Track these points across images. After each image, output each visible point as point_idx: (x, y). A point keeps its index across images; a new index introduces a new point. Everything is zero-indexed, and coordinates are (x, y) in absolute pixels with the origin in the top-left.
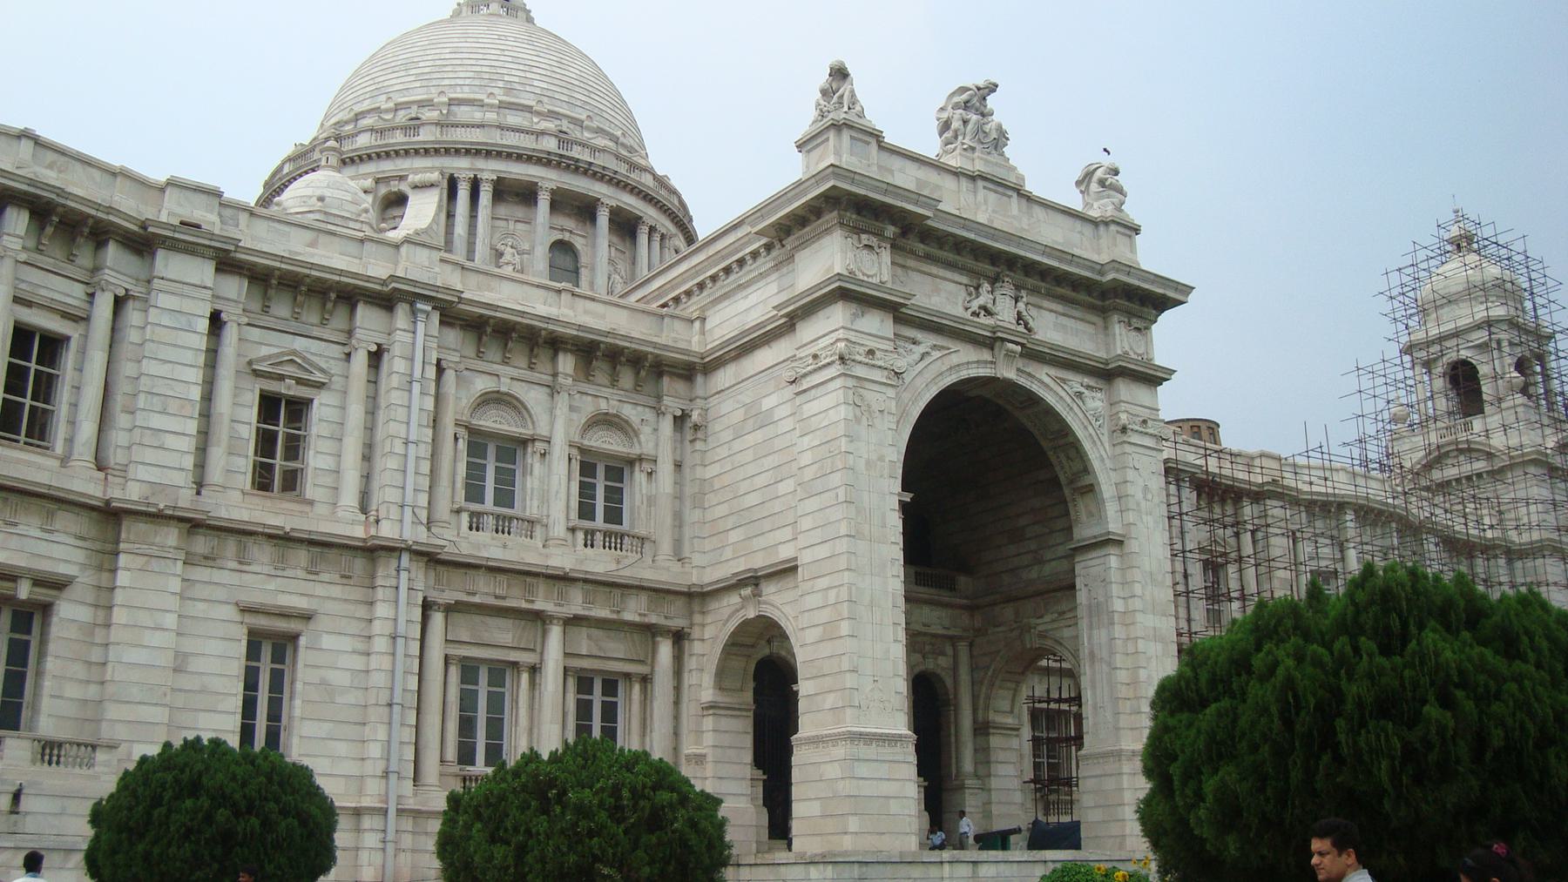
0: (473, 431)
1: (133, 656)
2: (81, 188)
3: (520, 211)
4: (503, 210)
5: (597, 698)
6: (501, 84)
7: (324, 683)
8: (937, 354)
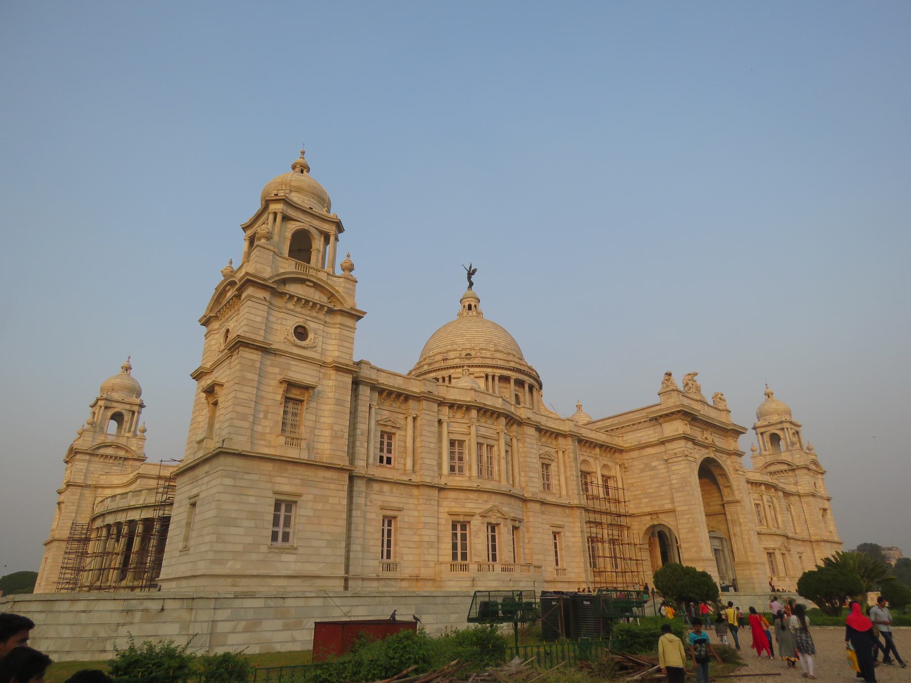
3: (504, 385)
4: (500, 385)
8: (699, 452)
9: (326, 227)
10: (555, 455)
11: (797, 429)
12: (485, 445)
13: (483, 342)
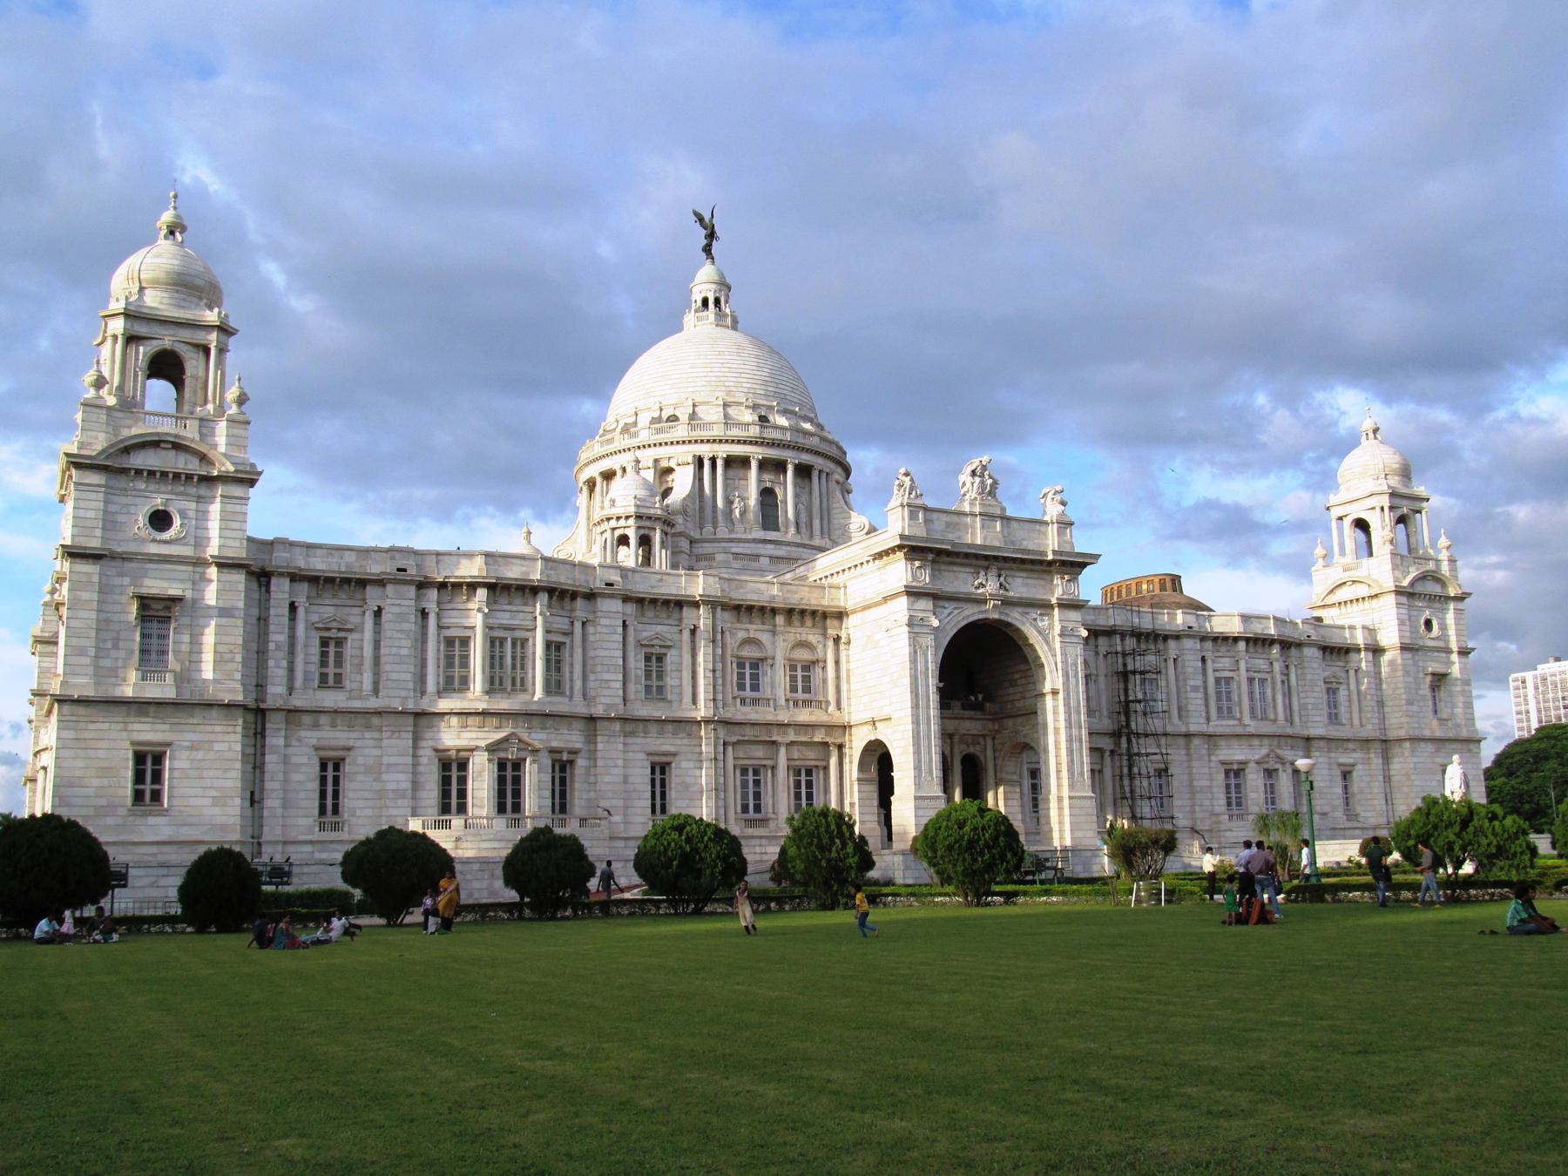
0: (737, 657)
1: (607, 779)
2: (564, 579)
3: (741, 473)
4: (731, 473)
5: (803, 778)
6: (723, 388)
7: (683, 782)
8: (956, 612)
9: (200, 337)
10: (676, 637)
11: (1416, 505)
12: (509, 639)
13: (703, 388)
